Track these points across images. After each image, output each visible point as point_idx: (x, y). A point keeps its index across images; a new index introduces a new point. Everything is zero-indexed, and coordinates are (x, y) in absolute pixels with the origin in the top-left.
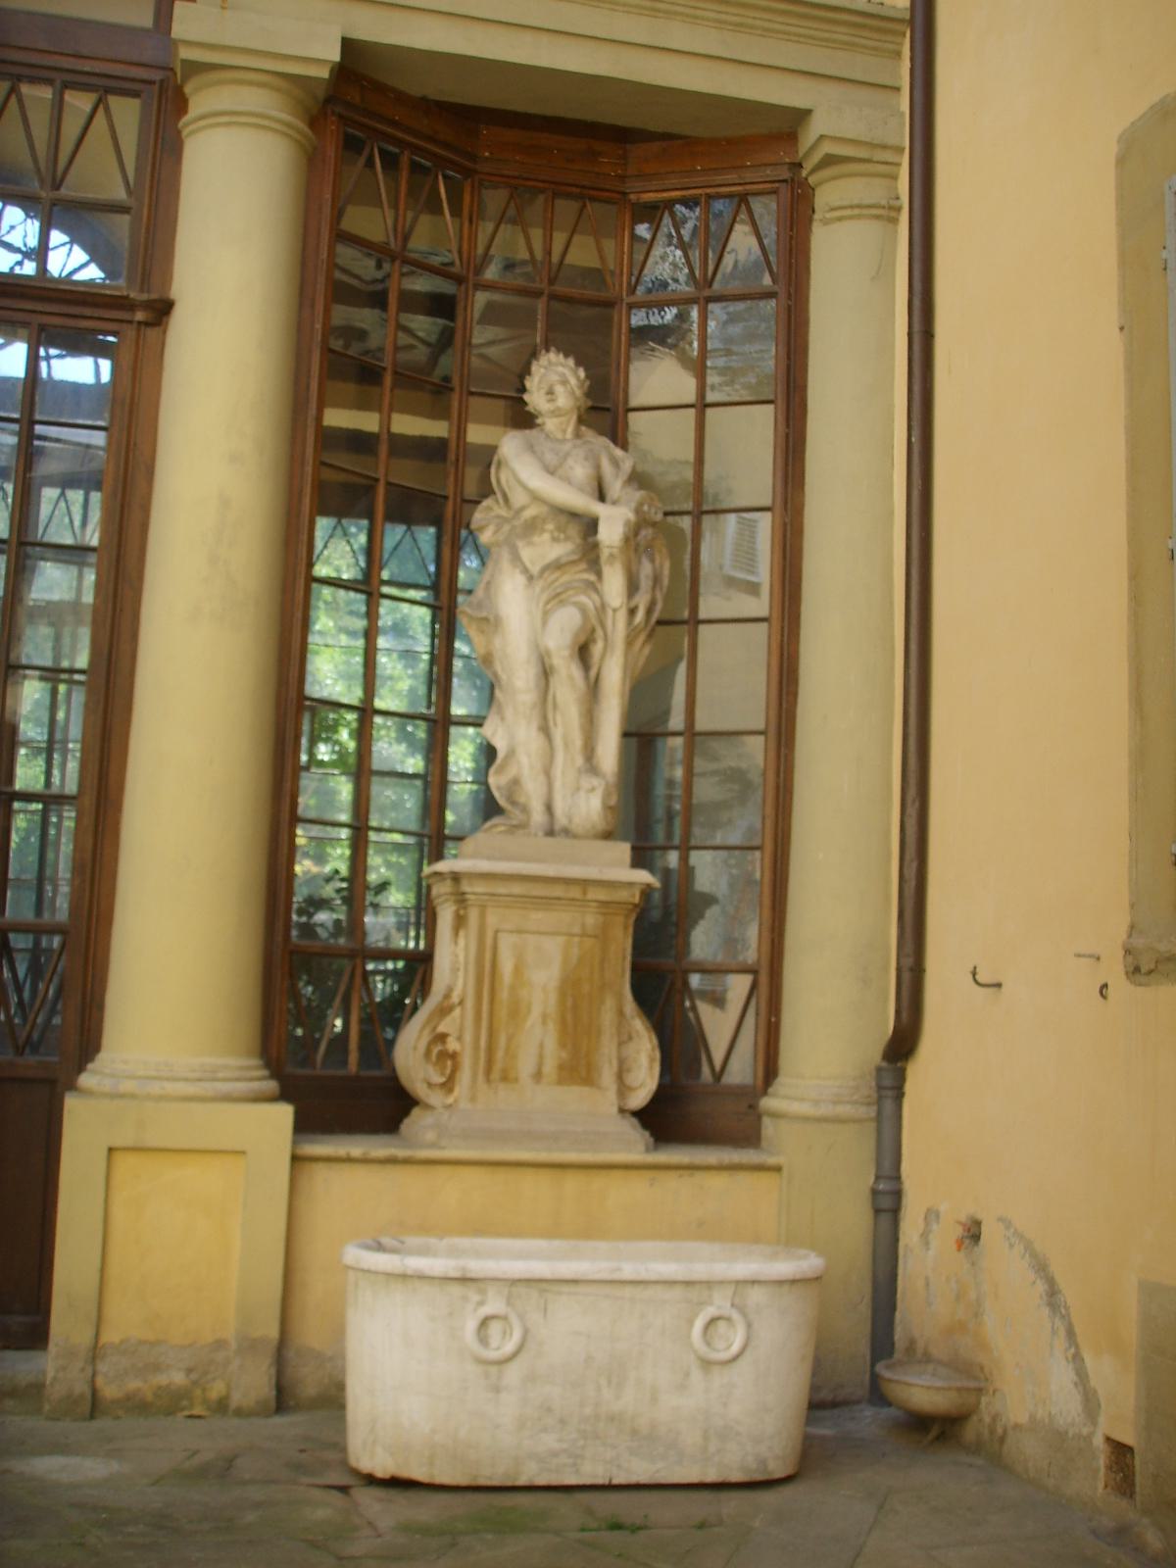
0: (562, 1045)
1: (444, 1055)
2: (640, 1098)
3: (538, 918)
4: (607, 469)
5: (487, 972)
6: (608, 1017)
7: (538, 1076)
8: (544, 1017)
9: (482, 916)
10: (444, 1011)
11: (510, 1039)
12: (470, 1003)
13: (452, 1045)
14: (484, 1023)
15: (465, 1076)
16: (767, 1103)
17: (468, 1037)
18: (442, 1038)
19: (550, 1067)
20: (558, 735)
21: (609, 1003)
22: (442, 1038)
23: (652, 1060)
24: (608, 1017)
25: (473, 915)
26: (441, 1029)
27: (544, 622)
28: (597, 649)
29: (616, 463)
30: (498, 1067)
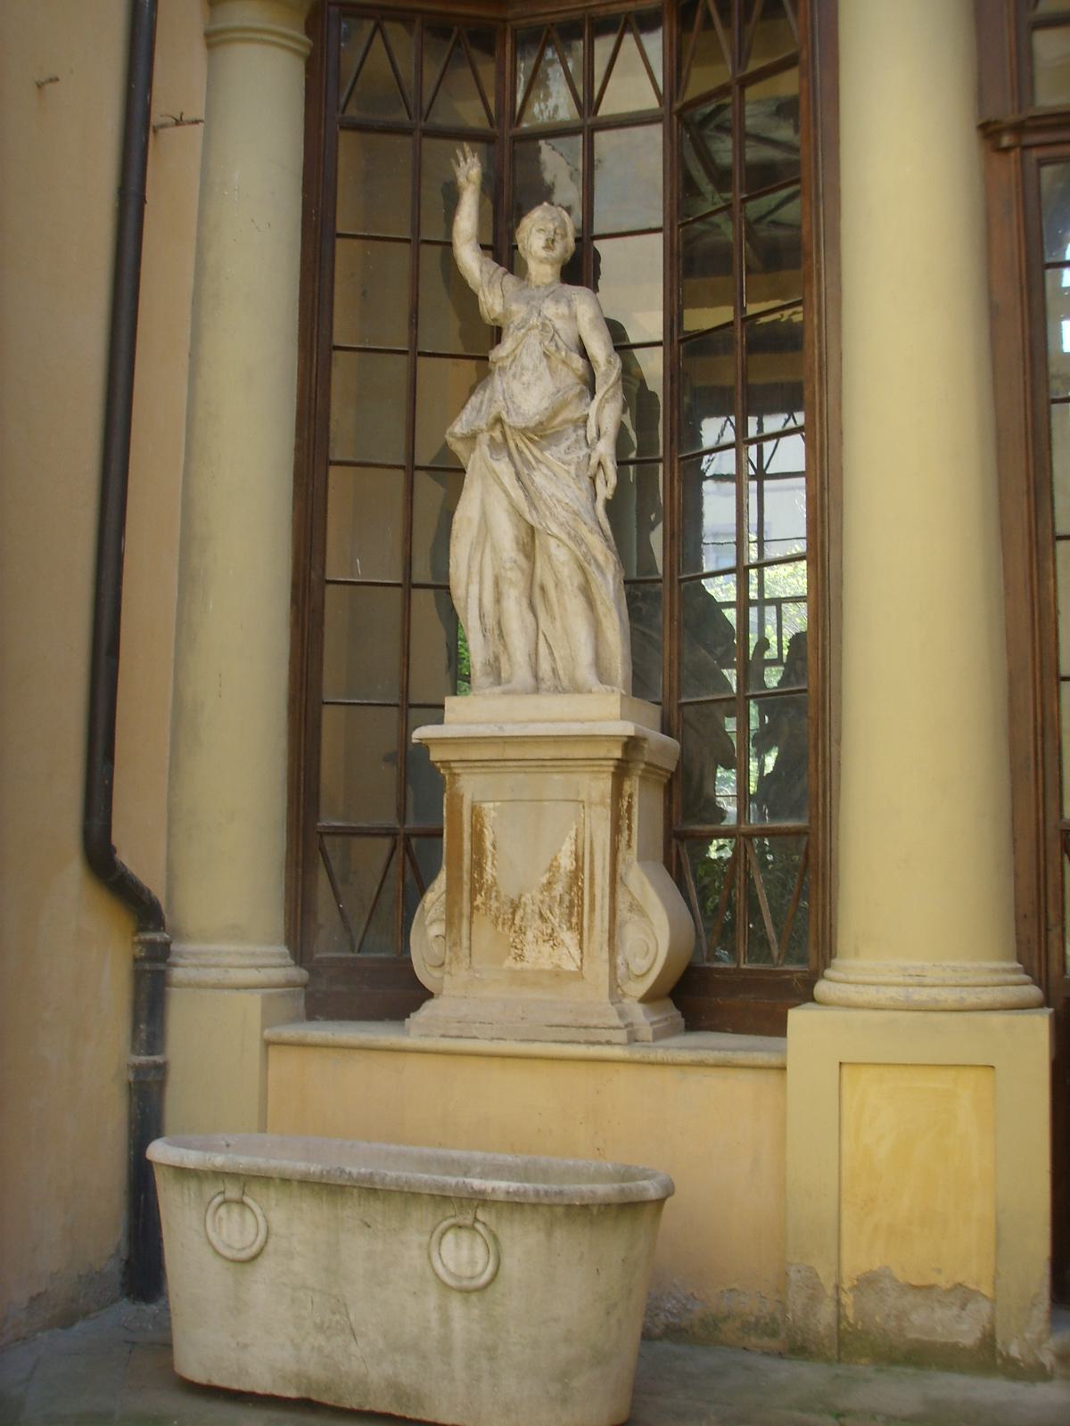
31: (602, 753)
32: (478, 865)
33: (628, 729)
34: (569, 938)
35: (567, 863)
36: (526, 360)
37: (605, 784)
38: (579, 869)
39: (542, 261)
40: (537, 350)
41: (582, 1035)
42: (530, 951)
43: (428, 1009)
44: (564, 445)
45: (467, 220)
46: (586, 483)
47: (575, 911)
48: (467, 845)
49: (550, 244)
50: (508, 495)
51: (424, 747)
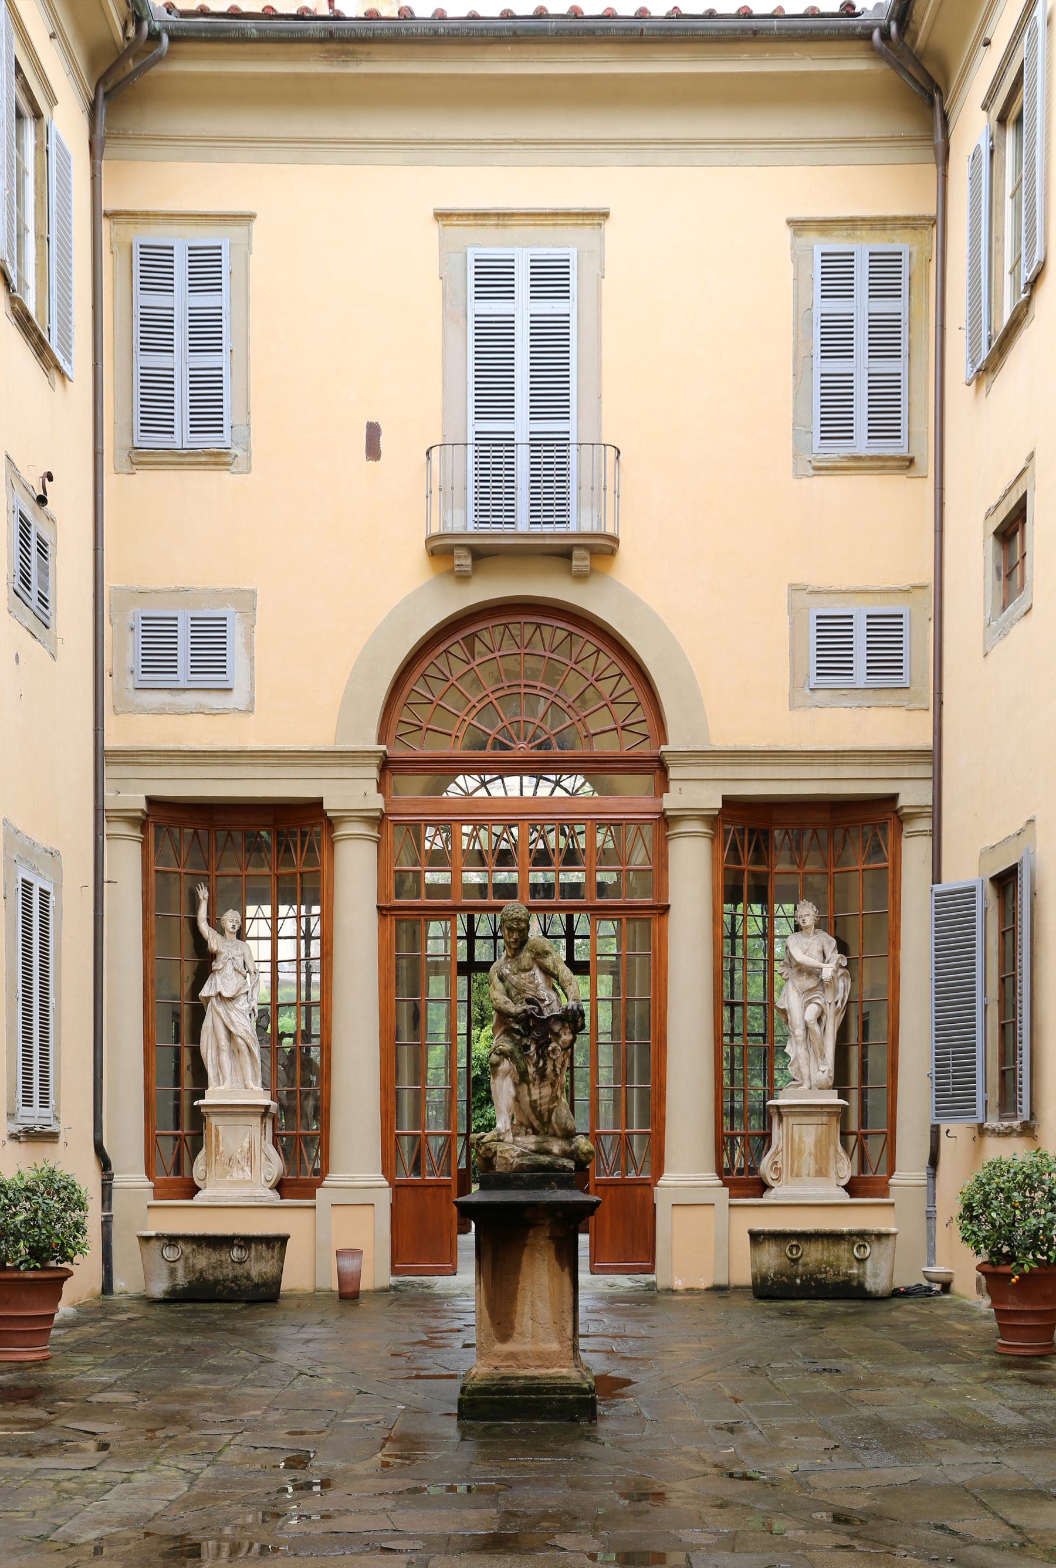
0: (816, 1162)
1: (776, 1169)
2: (844, 1182)
3: (806, 1120)
4: (826, 948)
5: (790, 1140)
6: (832, 1153)
7: (809, 1175)
8: (810, 1154)
9: (788, 1120)
10: (776, 1154)
11: (798, 1162)
12: (784, 1150)
13: (779, 1165)
14: (790, 1157)
15: (784, 1175)
16: (891, 1181)
17: (784, 1162)
18: (776, 1163)
19: (812, 1172)
20: (811, 1051)
21: (832, 1148)
22: (776, 1163)
23: (848, 1167)
24: (832, 1153)
25: (785, 1119)
26: (775, 1160)
27: (805, 1009)
28: (824, 1018)
29: (830, 943)
30: (795, 1172)
31: (258, 1110)
32: (217, 1146)
33: (267, 1101)
34: (247, 1169)
35: (246, 1145)
36: (227, 971)
37: (259, 1119)
38: (250, 1147)
39: (231, 933)
40: (231, 968)
41: (253, 1199)
42: (235, 1175)
43: (200, 1194)
44: (241, 1003)
45: (203, 913)
46: (248, 1016)
47: (250, 1160)
48: (213, 1139)
49: (234, 927)
50: (222, 1019)
51: (199, 1107)
